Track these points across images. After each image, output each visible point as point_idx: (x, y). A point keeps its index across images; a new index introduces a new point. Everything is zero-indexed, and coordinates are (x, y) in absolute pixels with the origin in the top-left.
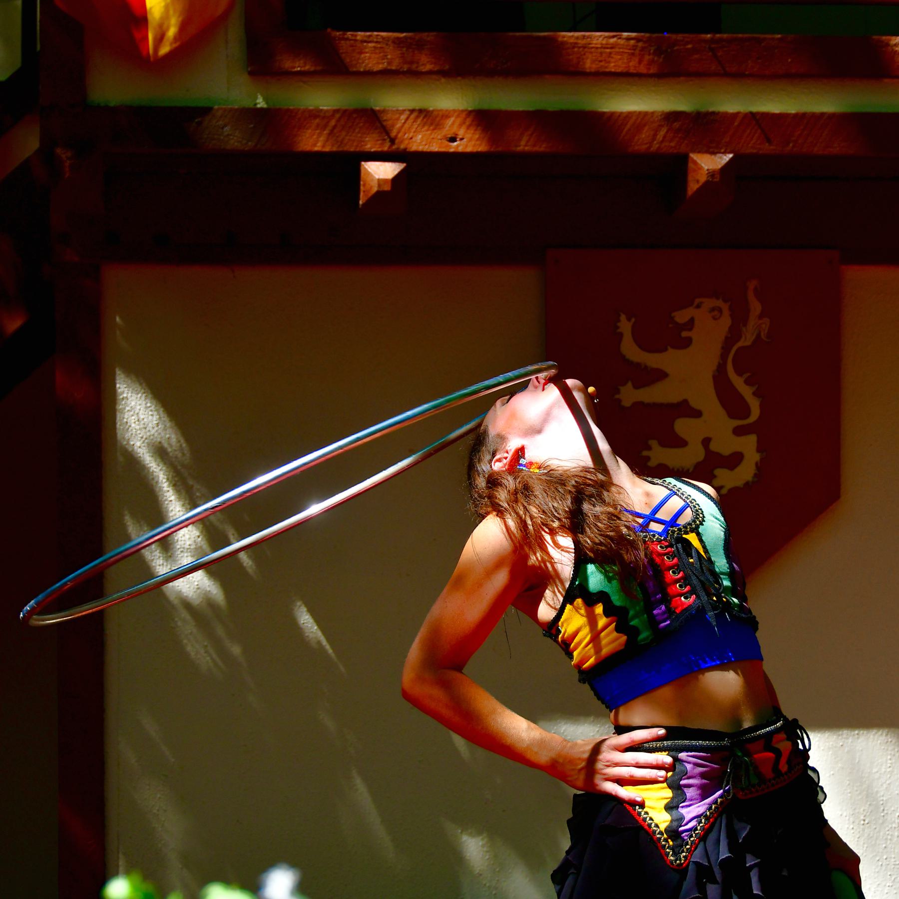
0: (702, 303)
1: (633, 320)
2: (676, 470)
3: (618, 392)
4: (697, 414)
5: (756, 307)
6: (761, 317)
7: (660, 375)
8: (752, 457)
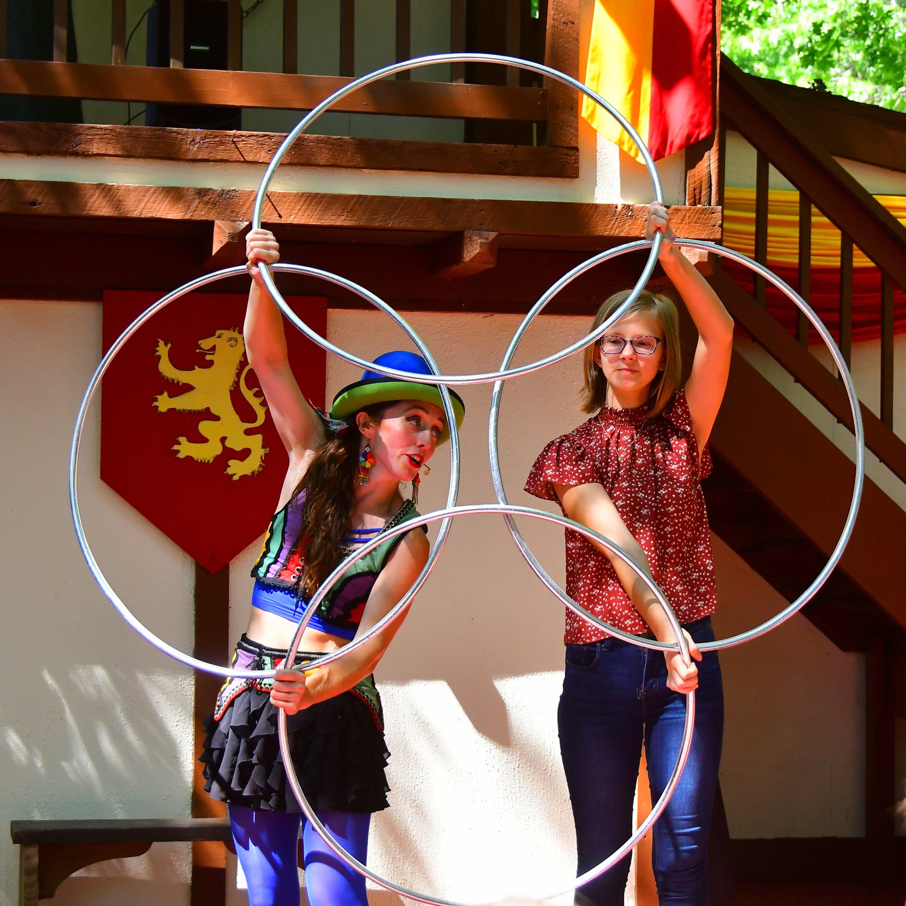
0: (221, 334)
1: (169, 345)
2: (199, 461)
3: (156, 400)
4: (217, 418)
7: (188, 388)
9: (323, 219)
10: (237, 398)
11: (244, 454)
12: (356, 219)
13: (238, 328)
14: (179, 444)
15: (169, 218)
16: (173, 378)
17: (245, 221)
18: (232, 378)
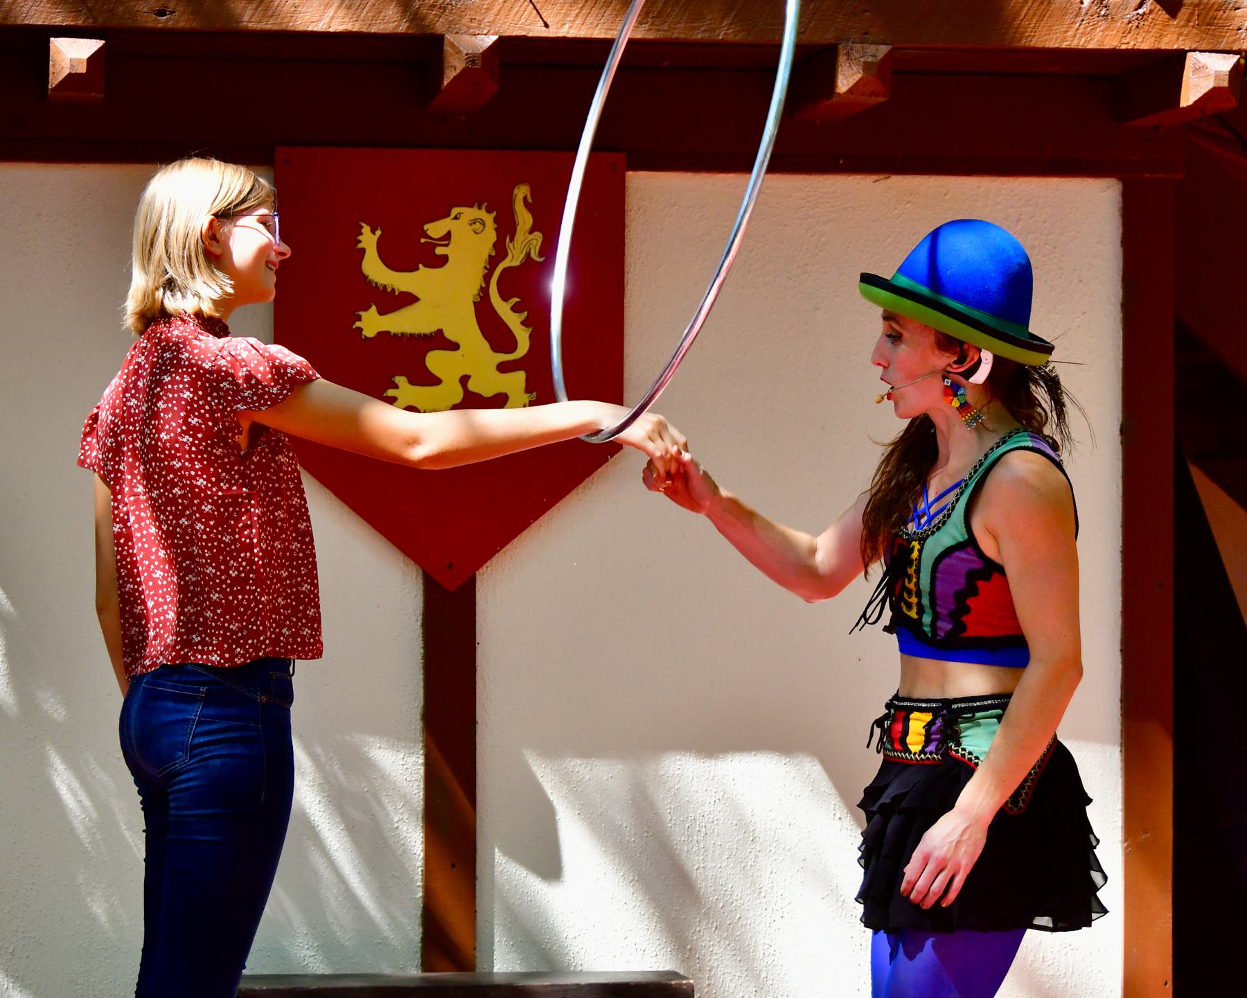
0: (459, 214)
1: (378, 233)
3: (359, 318)
4: (454, 346)
6: (531, 232)
7: (408, 299)
9: (614, 30)
10: (484, 311)
12: (666, 28)
13: (485, 204)
14: (396, 387)
15: (373, 31)
16: (385, 282)
17: (493, 34)
18: (478, 282)
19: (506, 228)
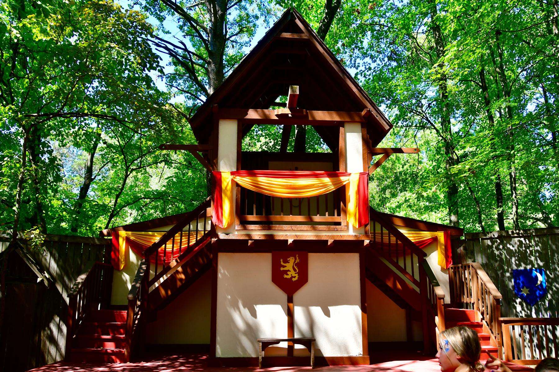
5: (297, 258)
7: (286, 266)
8: (297, 277)
11: (295, 277)
19: (296, 259)
